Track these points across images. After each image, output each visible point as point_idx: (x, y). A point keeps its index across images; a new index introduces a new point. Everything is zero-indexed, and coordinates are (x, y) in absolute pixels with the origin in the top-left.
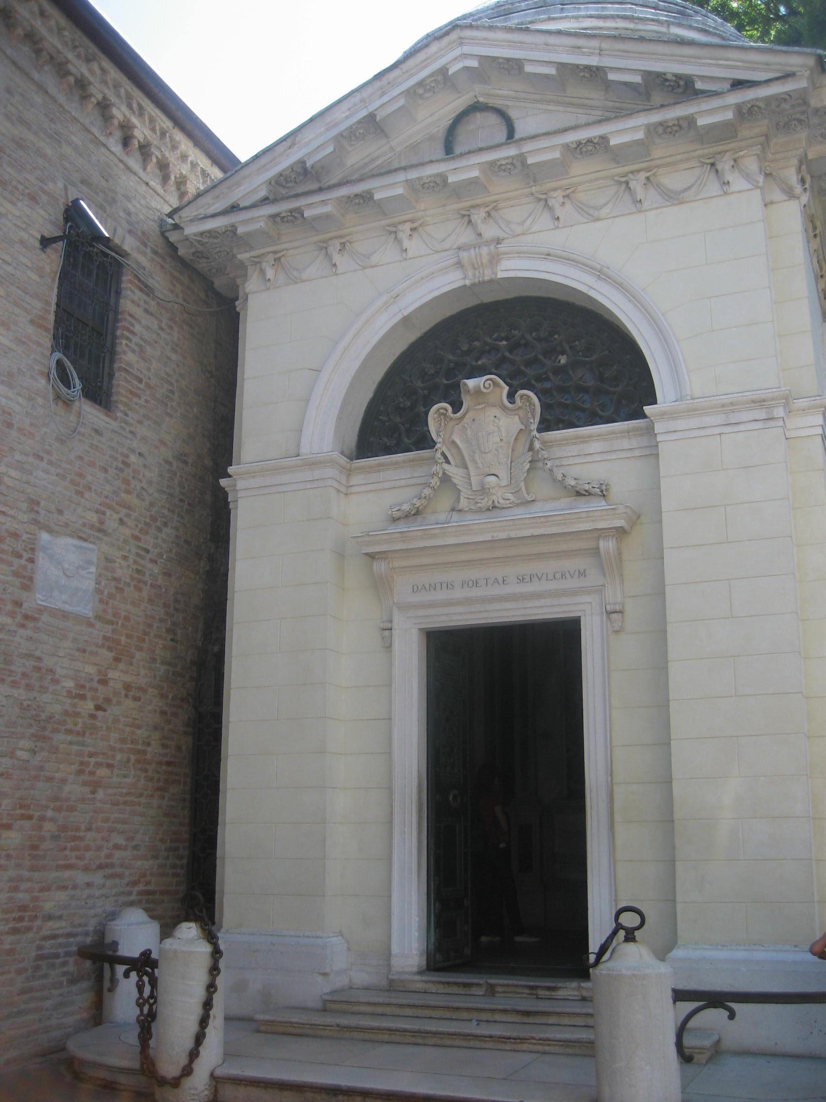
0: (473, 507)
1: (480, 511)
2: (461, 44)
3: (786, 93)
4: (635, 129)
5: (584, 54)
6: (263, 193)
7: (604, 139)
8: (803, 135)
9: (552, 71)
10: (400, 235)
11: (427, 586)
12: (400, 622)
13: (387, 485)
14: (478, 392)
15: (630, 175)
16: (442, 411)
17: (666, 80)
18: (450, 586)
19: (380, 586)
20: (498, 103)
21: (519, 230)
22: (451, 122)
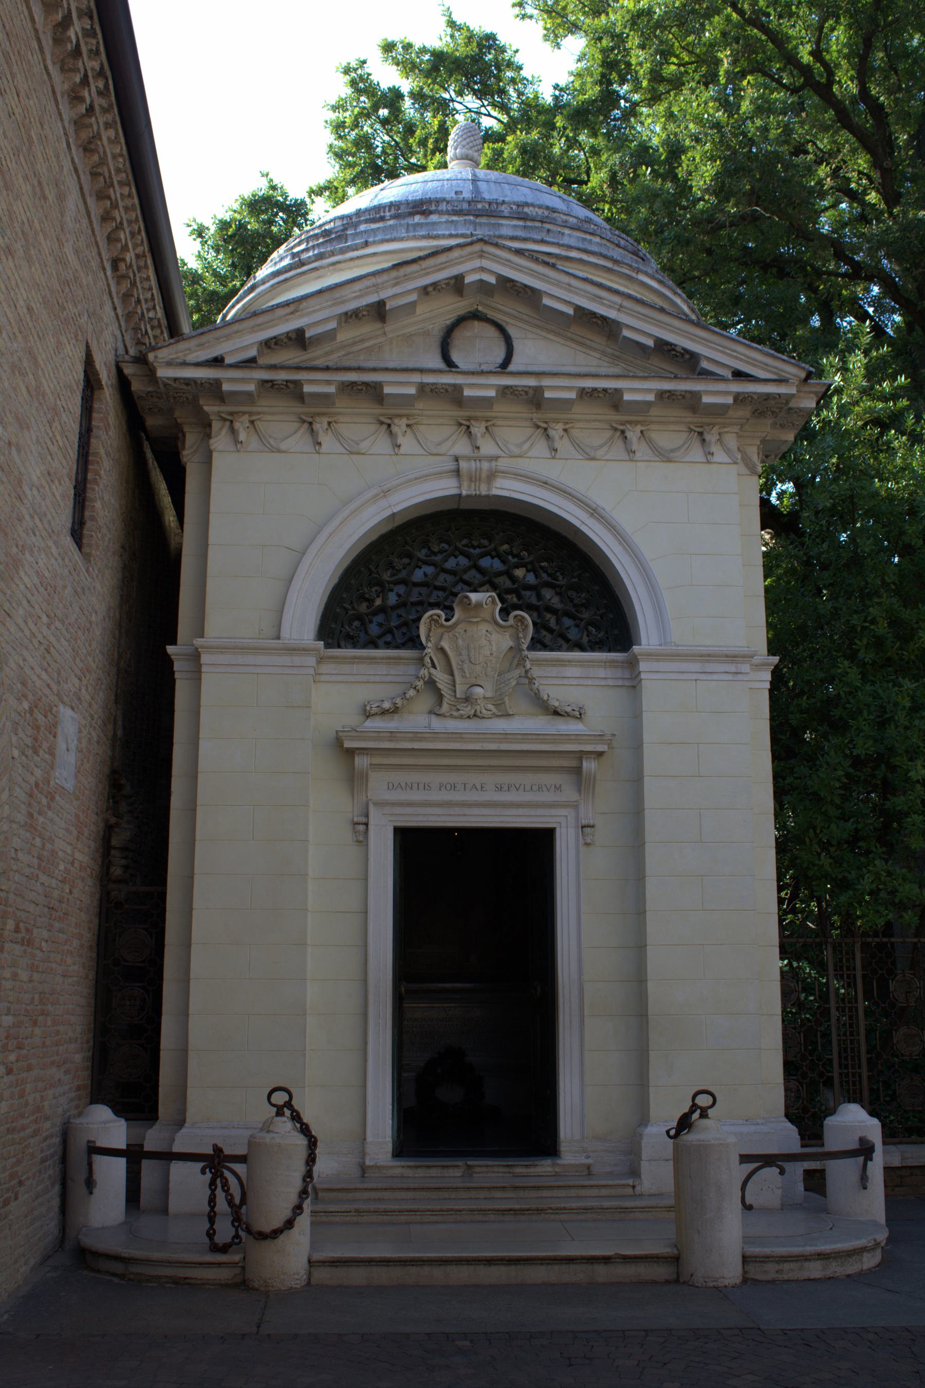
0: (455, 713)
1: (461, 717)
2: (481, 257)
3: (779, 394)
4: (648, 391)
5: (603, 304)
6: (253, 352)
7: (618, 392)
8: (769, 422)
9: (570, 311)
10: (395, 429)
11: (403, 785)
13: (359, 678)
14: (479, 605)
15: (628, 426)
16: (435, 617)
17: (674, 350)
18: (427, 787)
20: (498, 317)
21: (516, 451)
22: (448, 322)
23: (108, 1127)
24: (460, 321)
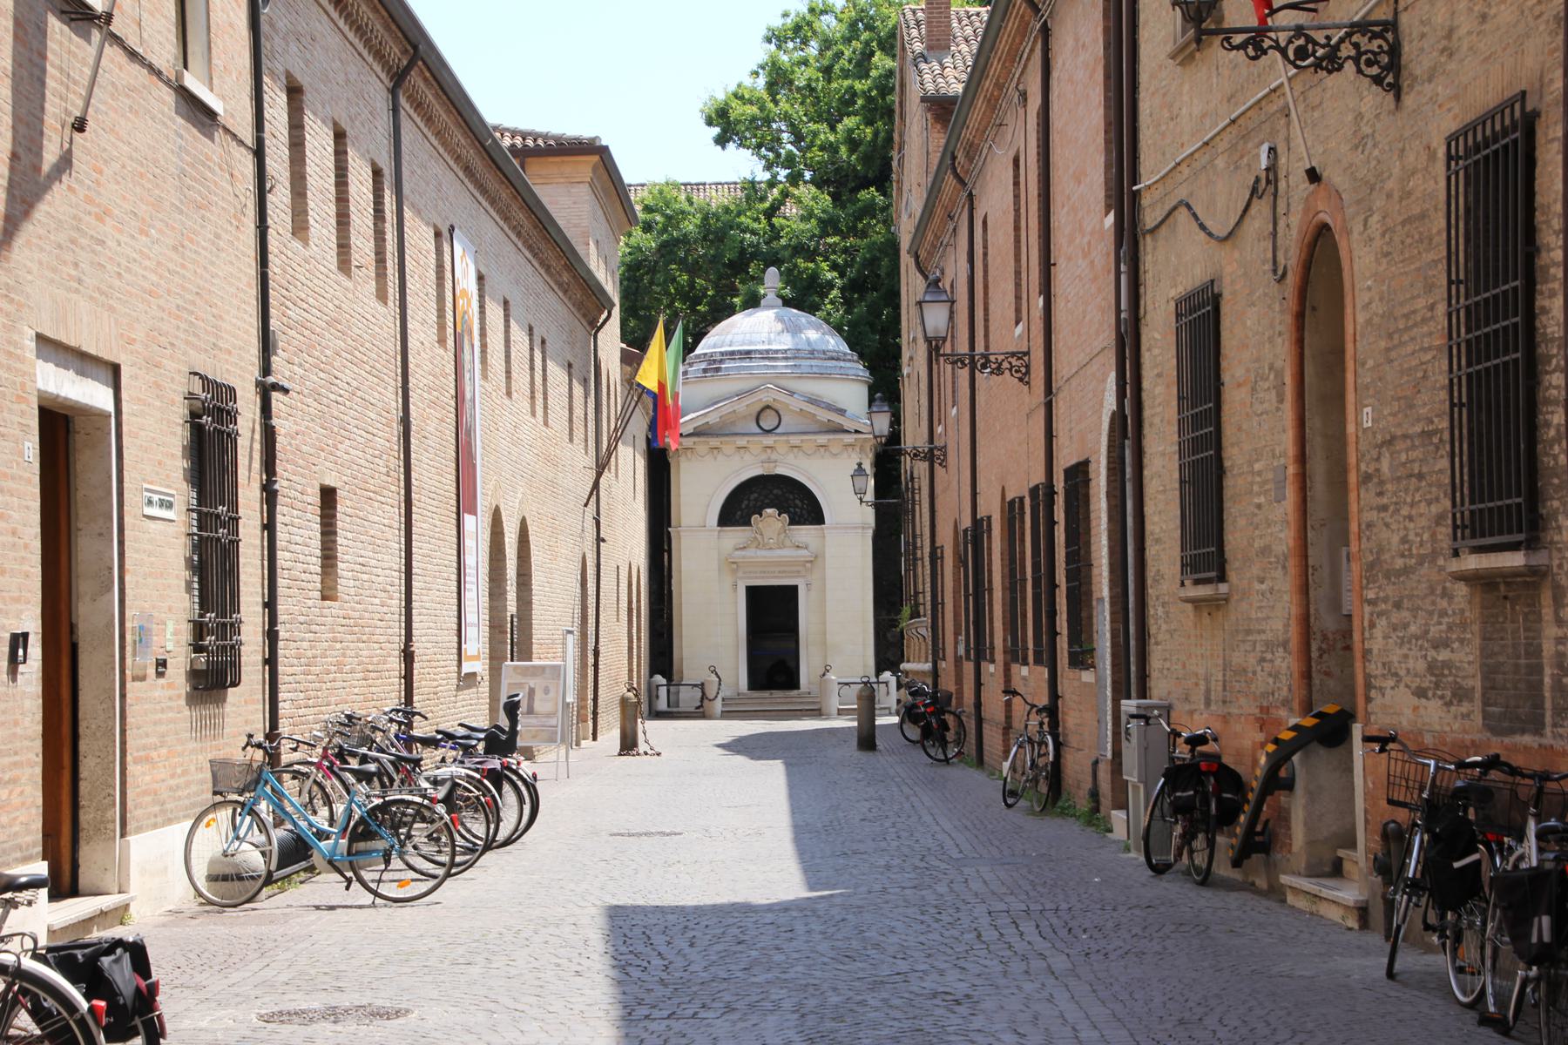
19: (734, 572)
23: (659, 679)
24: (763, 410)
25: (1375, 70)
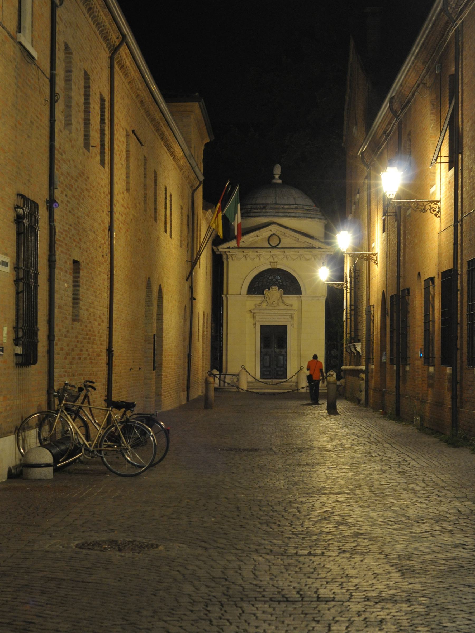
12: (257, 324)
18: (266, 318)
22: (269, 235)
25: (435, 212)
